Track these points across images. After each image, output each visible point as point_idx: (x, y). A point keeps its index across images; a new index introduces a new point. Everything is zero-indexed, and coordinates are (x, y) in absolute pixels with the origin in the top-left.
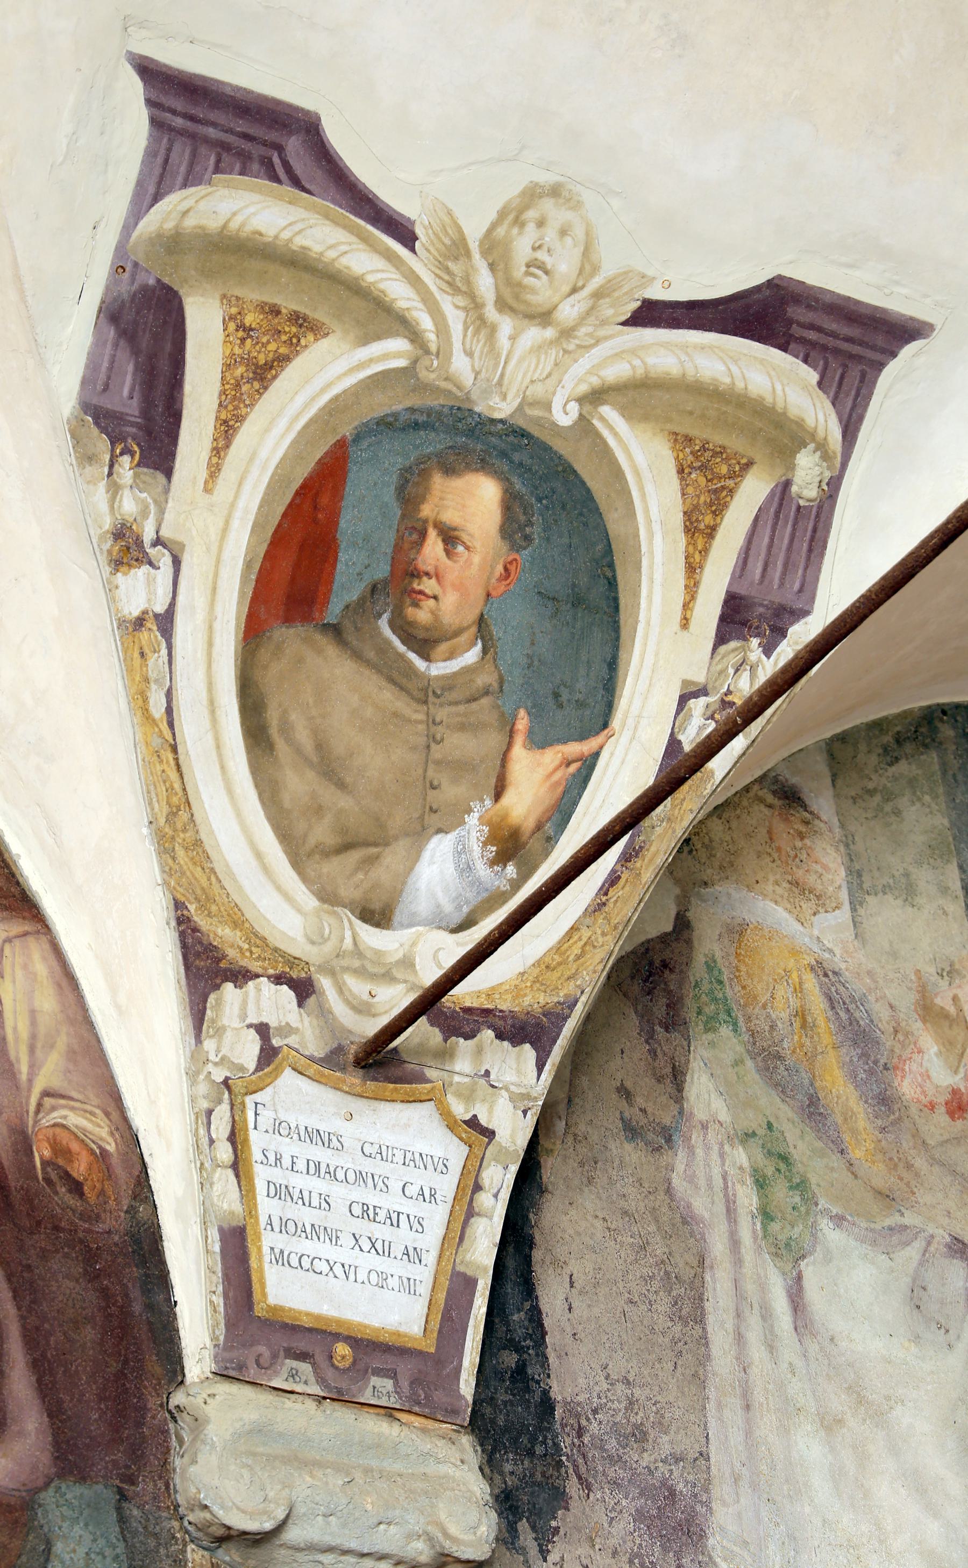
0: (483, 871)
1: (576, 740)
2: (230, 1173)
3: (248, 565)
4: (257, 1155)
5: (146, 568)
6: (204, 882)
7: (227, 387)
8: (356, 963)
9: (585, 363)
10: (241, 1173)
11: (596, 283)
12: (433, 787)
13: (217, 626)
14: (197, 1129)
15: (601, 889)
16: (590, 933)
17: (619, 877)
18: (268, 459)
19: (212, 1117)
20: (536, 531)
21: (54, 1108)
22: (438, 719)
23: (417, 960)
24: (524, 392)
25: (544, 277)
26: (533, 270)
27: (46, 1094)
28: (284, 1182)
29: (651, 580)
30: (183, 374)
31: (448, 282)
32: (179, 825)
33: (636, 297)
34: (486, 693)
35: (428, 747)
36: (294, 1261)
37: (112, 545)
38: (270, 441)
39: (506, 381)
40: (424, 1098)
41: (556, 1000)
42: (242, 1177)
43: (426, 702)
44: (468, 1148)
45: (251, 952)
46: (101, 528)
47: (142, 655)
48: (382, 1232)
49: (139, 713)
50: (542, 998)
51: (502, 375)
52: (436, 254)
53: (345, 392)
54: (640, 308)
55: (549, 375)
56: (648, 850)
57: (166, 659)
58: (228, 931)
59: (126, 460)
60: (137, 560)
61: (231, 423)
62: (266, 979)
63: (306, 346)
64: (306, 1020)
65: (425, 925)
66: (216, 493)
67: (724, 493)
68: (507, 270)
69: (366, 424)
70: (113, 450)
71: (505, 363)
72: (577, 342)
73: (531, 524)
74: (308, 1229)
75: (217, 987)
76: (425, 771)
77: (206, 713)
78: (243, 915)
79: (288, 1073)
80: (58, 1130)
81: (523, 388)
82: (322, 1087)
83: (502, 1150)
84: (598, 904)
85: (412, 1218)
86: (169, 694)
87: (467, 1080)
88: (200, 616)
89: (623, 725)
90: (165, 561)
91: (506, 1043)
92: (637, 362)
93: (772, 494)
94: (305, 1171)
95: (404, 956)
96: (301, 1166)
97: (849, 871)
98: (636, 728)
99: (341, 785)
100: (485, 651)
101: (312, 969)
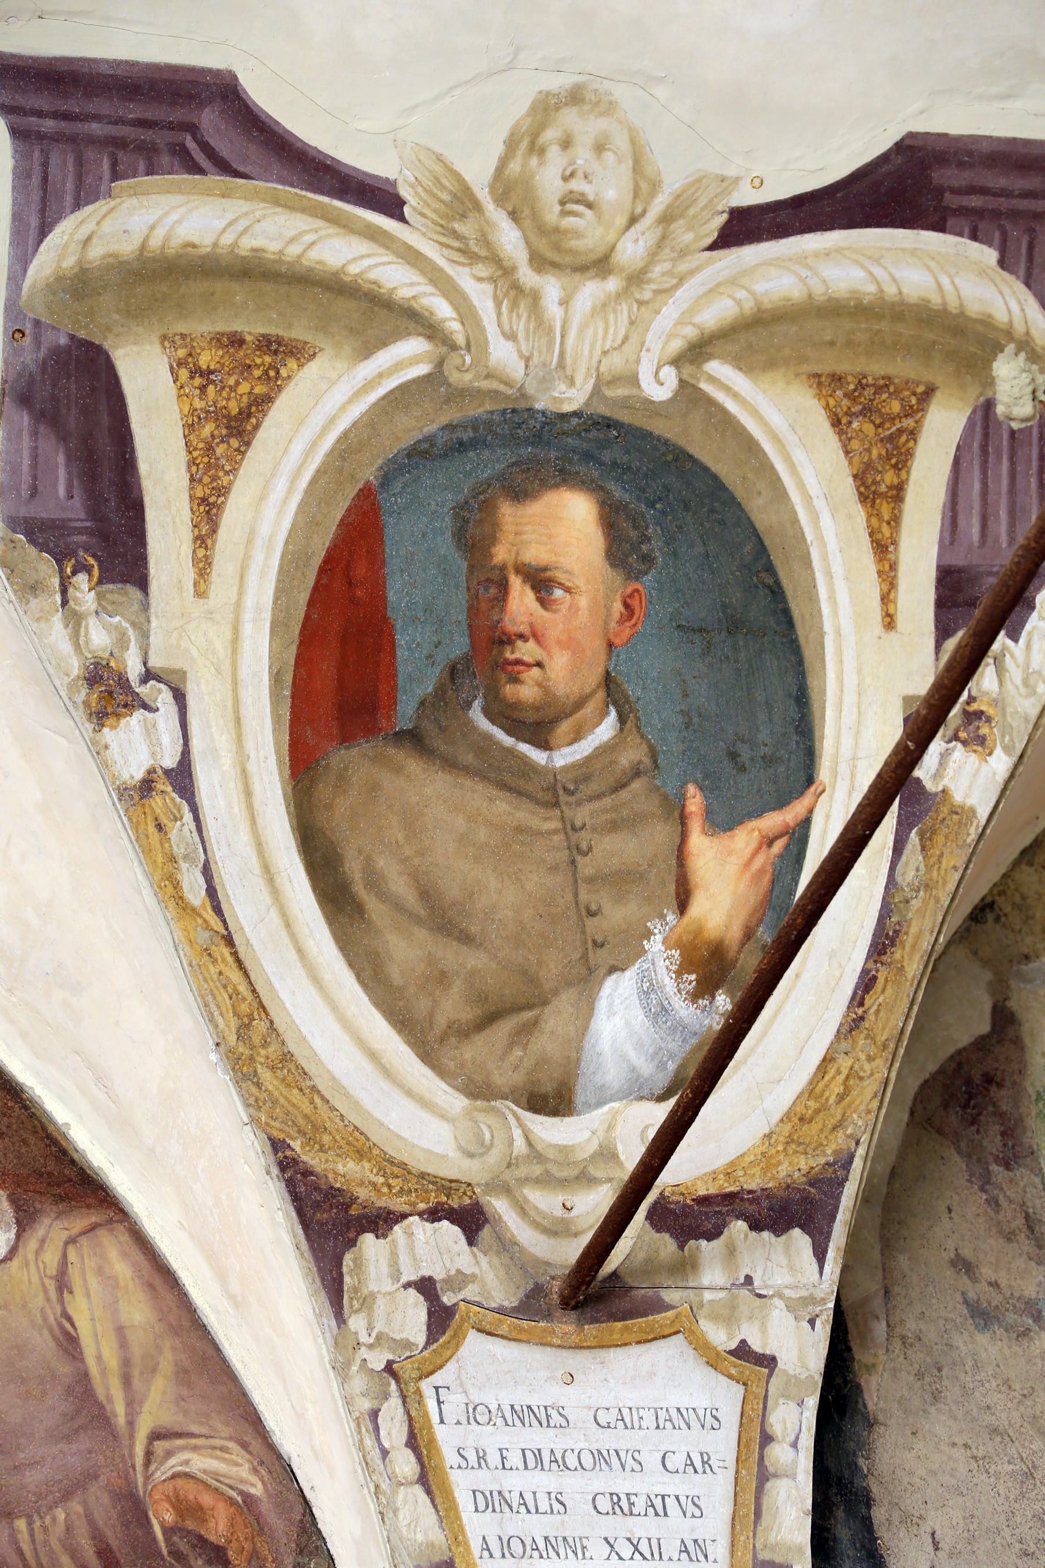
0: (684, 1010)
1: (774, 809)
2: (418, 1491)
3: (276, 679)
4: (450, 1458)
5: (139, 714)
6: (306, 1107)
7: (196, 454)
8: (537, 1170)
10: (434, 1487)
11: (659, 204)
12: (592, 914)
13: (252, 767)
14: (361, 1441)
15: (853, 998)
16: (851, 1061)
17: (875, 978)
18: (272, 536)
19: (380, 1420)
20: (656, 546)
21: (169, 1454)
22: (578, 823)
23: (620, 1148)
24: (598, 369)
25: (588, 212)
26: (570, 207)
27: (156, 1436)
28: (496, 1487)
29: (829, 575)
30: (133, 451)
31: (459, 250)
32: (257, 1040)
33: (720, 208)
35: (573, 862)
37: (88, 694)
38: (269, 511)
39: (569, 361)
40: (667, 1331)
41: (822, 1160)
42: (437, 1493)
43: (556, 804)
44: (741, 1389)
45: (389, 1186)
46: (68, 675)
47: (160, 827)
48: (644, 1527)
49: (172, 904)
51: (562, 354)
52: (434, 216)
53: (355, 424)
54: (729, 222)
56: (906, 933)
57: (193, 826)
58: (351, 1165)
59: (82, 579)
60: (125, 706)
61: (212, 500)
62: (417, 1217)
63: (289, 377)
64: (484, 1261)
65: (621, 1099)
66: (212, 594)
67: (904, 438)
68: (535, 215)
69: (393, 461)
70: (61, 571)
71: (563, 337)
72: (653, 286)
73: (646, 539)
74: (541, 1544)
75: (352, 1243)
76: (576, 895)
77: (260, 883)
78: (368, 1139)
79: (472, 1336)
80: (180, 1482)
81: (595, 364)
82: (524, 1348)
83: (792, 1381)
84: (854, 1020)
85: (683, 1499)
86: (207, 871)
87: (722, 1295)
88: (227, 760)
89: (835, 774)
90: (164, 698)
91: (766, 1234)
92: (742, 294)
93: (971, 423)
94: (521, 1466)
95: (600, 1146)
96: (514, 1459)
98: (853, 775)
99: (466, 939)
100: (622, 719)
101: (478, 1190)
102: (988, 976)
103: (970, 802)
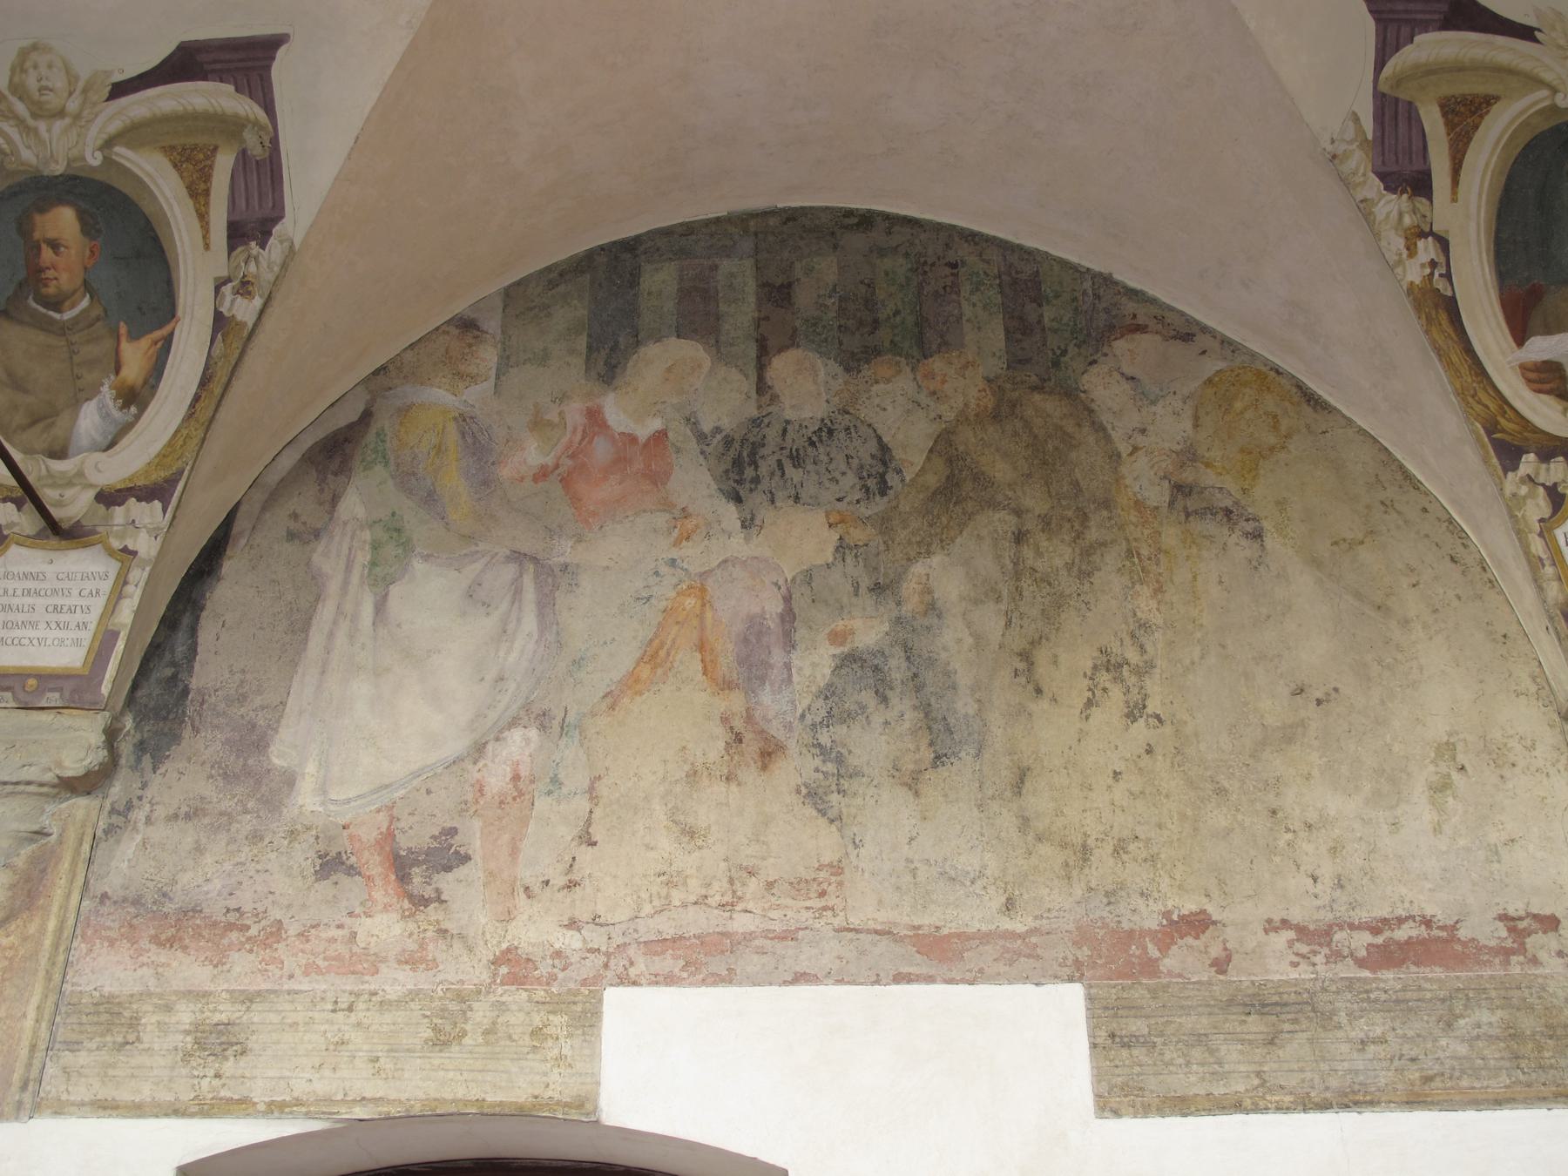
0: (117, 414)
8: (50, 481)
9: (93, 131)
11: (81, 85)
12: (79, 378)
29: (179, 230)
34: (98, 319)
35: (71, 358)
36: (9, 642)
43: (64, 335)
44: (120, 564)
48: (63, 618)
50: (163, 474)
54: (112, 89)
55: (77, 143)
64: (23, 517)
76: (72, 370)
89: (184, 313)
91: (143, 503)
93: (237, 159)
96: (19, 592)
97: (501, 357)
99: (26, 391)
100: (92, 298)
102: (368, 397)
103: (244, 319)
